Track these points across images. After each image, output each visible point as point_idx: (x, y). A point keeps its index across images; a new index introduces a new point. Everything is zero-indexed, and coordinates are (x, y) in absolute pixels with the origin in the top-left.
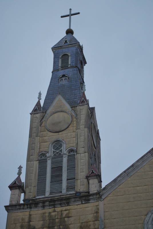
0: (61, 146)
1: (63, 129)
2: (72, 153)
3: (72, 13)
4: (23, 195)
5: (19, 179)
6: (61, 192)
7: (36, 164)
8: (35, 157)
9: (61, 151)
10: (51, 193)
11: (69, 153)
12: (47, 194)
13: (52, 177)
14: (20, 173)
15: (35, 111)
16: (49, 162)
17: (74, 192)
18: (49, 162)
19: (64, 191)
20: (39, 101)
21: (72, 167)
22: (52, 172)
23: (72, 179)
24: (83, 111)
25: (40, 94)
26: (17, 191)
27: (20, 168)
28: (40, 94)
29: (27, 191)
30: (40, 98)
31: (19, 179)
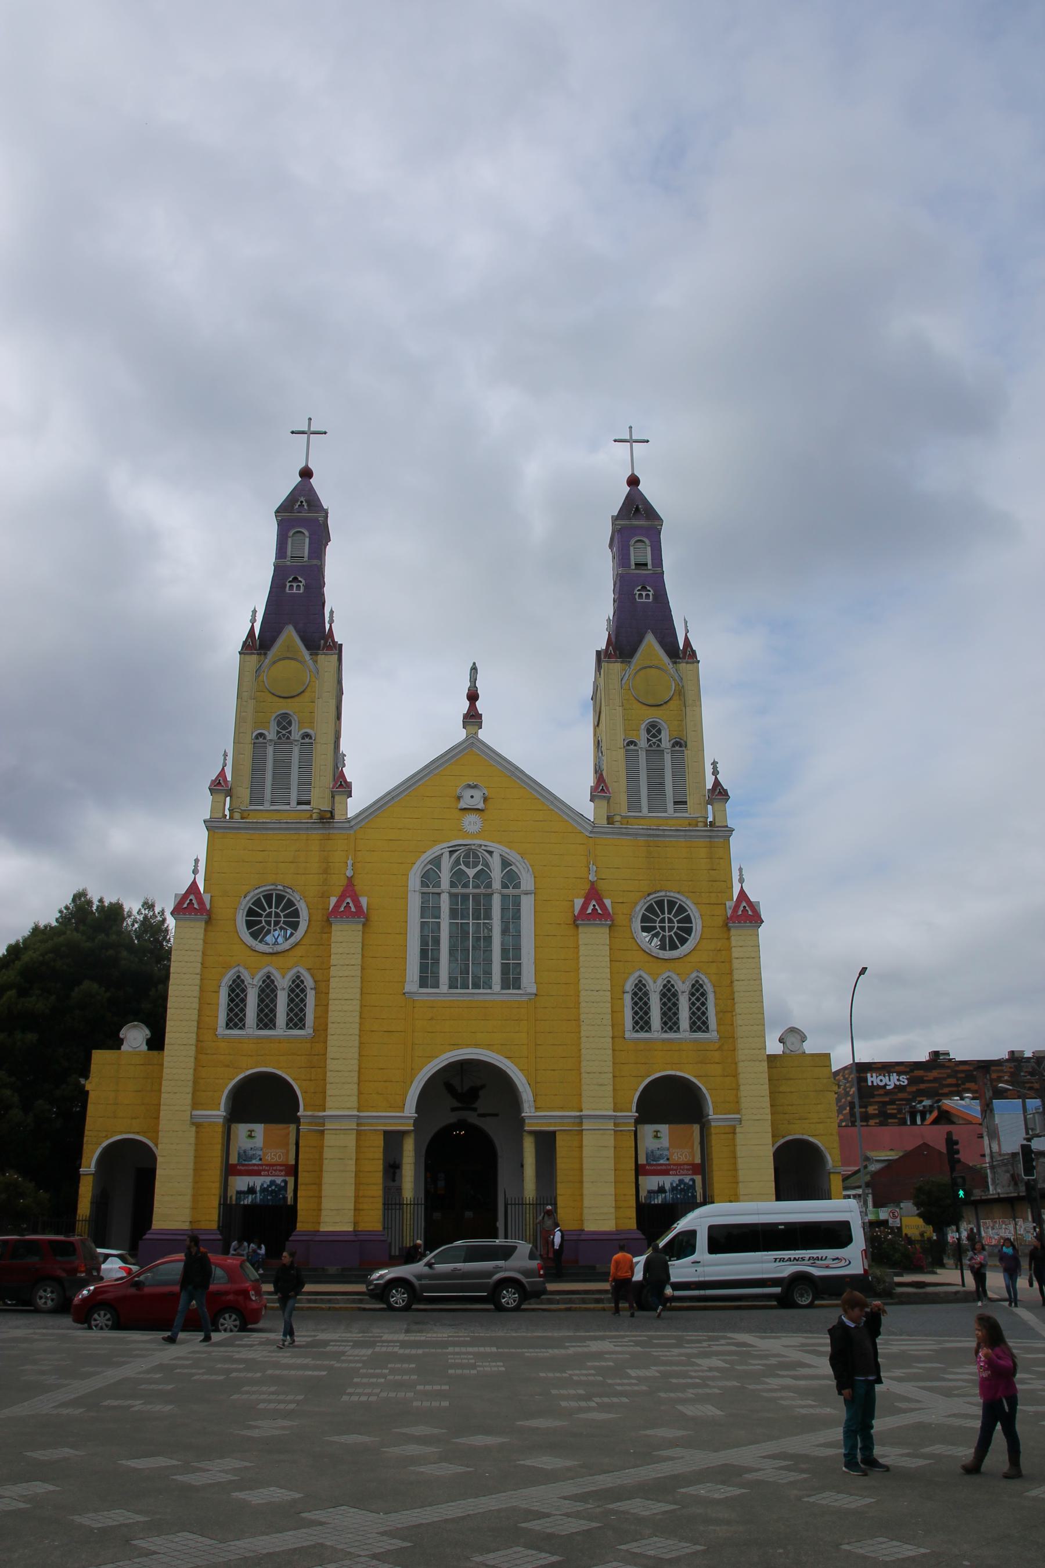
0: (290, 723)
1: (295, 694)
2: (307, 740)
3: (312, 429)
4: (228, 798)
5: (222, 773)
6: (289, 804)
7: (248, 749)
8: (248, 738)
11: (303, 738)
12: (267, 806)
16: (270, 750)
18: (270, 750)
20: (252, 628)
21: (306, 765)
22: (275, 767)
23: (305, 784)
24: (326, 660)
25: (254, 612)
26: (220, 797)
27: (225, 755)
28: (254, 612)
29: (234, 791)
30: (253, 621)
31: (222, 773)
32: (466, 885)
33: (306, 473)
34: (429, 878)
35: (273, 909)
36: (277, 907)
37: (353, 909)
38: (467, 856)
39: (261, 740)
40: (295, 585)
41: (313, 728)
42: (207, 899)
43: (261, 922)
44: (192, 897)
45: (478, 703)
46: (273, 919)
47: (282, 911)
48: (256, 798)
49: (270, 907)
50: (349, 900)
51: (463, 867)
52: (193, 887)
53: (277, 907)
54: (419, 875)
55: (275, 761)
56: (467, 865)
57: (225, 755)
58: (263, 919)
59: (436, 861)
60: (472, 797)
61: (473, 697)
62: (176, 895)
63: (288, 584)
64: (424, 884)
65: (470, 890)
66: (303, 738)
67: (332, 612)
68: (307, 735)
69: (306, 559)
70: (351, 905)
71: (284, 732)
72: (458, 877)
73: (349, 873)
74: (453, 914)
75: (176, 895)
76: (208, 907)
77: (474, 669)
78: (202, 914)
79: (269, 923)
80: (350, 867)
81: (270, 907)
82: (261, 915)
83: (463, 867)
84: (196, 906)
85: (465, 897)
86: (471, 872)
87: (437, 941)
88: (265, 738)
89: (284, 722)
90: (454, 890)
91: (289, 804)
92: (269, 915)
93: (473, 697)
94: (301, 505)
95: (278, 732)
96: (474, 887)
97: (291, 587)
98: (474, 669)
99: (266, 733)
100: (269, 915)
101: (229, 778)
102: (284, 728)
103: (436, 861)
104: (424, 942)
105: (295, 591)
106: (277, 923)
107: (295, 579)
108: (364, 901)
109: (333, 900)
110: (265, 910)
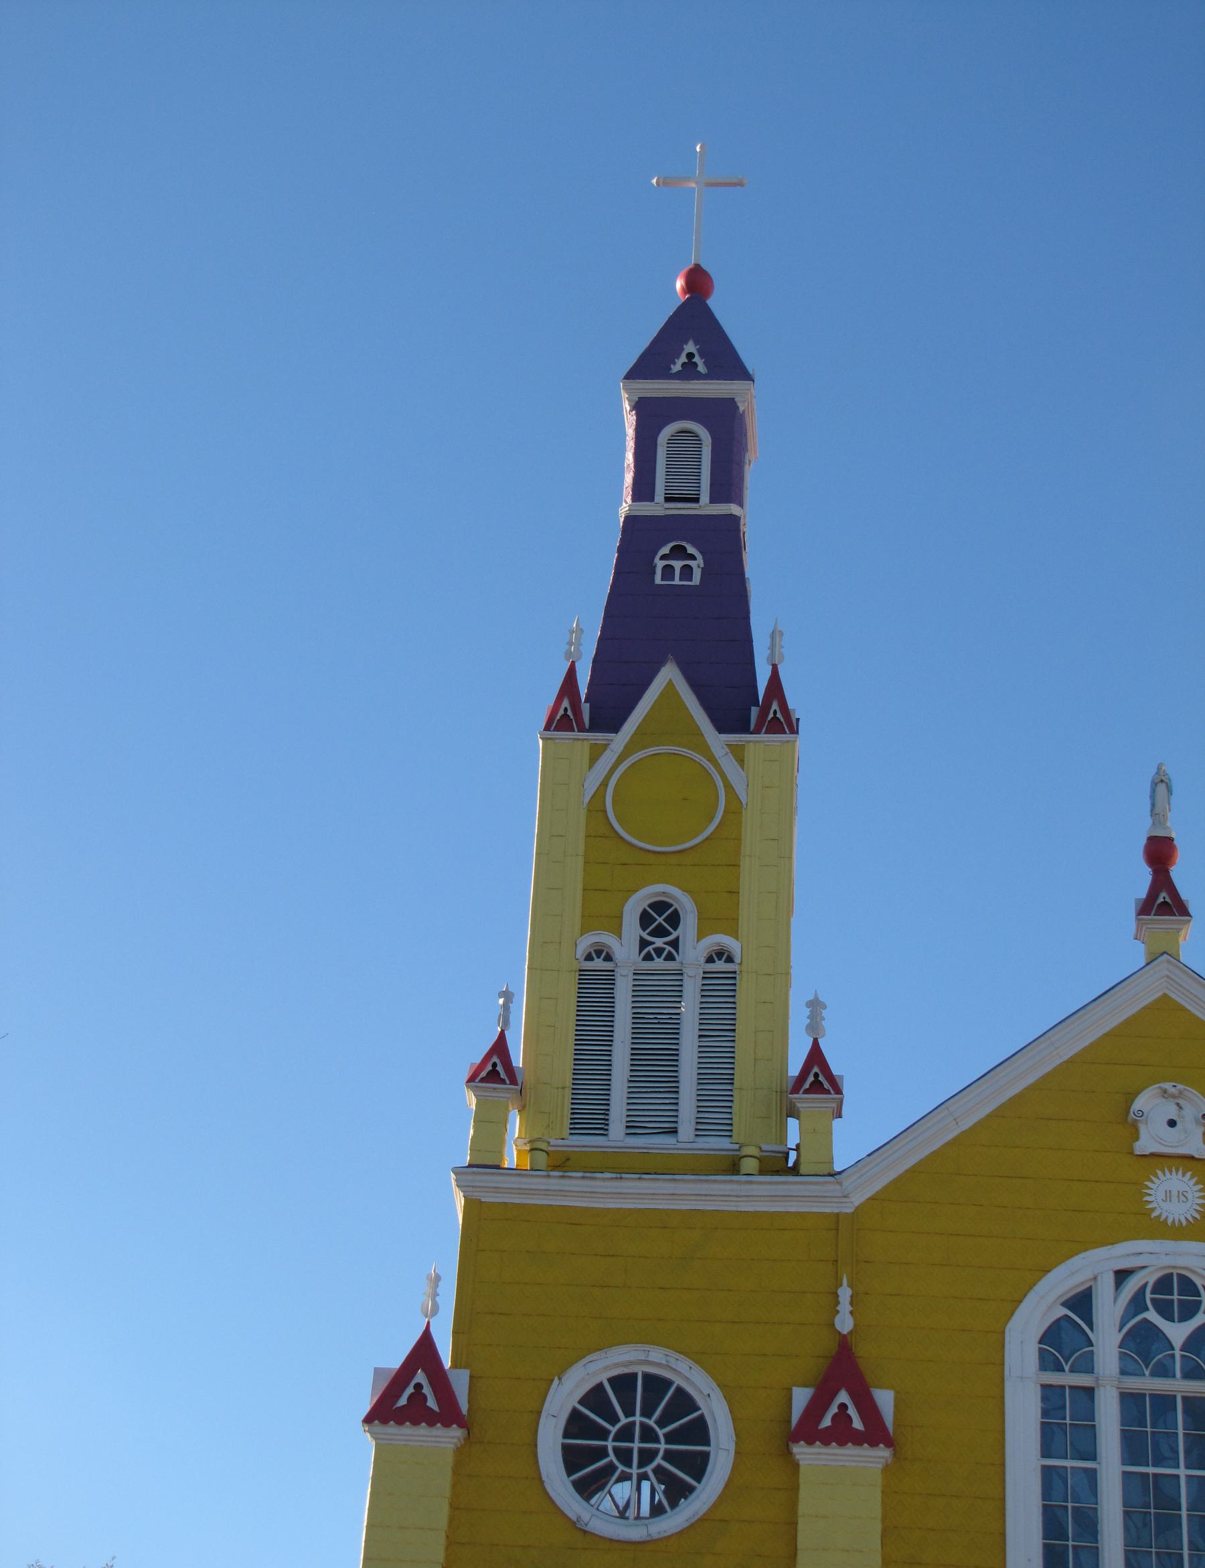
0: (674, 919)
2: (720, 965)
5: (500, 1047)
6: (674, 1131)
9: (675, 944)
10: (632, 1128)
13: (635, 1053)
14: (506, 1021)
15: (558, 723)
17: (724, 1143)
19: (686, 1129)
21: (720, 1028)
22: (637, 1033)
23: (718, 1078)
27: (508, 996)
31: (500, 1047)
32: (1163, 1371)
33: (698, 282)
34: (1065, 1341)
35: (638, 1418)
36: (647, 1413)
37: (857, 1424)
38: (1164, 1284)
39: (598, 964)
40: (677, 565)
41: (735, 935)
42: (460, 1383)
43: (603, 1453)
44: (420, 1377)
45: (1178, 874)
46: (636, 1445)
47: (662, 1423)
48: (589, 1116)
49: (629, 1412)
50: (843, 1397)
51: (1152, 1316)
52: (425, 1349)
53: (647, 1413)
54: (1037, 1328)
55: (636, 1017)
56: (1165, 1310)
57: (508, 996)
58: (610, 1444)
59: (1082, 1303)
60: (1172, 1123)
61: (1160, 853)
62: (378, 1372)
63: (660, 564)
64: (1048, 1363)
65: (1179, 1386)
66: (710, 960)
67: (774, 635)
68: (721, 954)
69: (705, 497)
70: (852, 1411)
71: (659, 942)
72: (1142, 1343)
73: (845, 1323)
74: (1133, 1448)
75: (378, 1372)
76: (464, 1407)
77: (1161, 782)
78: (447, 1425)
79: (625, 1456)
80: (845, 1306)
81: (629, 1412)
82: (604, 1434)
83: (1152, 1316)
84: (432, 1403)
85: (1164, 1403)
86: (1177, 1333)
87: (1089, 1524)
88: (608, 958)
89: (660, 920)
90: (1136, 1384)
91: (674, 1131)
92: (626, 1434)
93: (1160, 853)
94: (690, 365)
95: (644, 944)
96: (1187, 1375)
97: (668, 572)
98: (1161, 782)
99: (608, 939)
100: (626, 1434)
101: (518, 1060)
102: (660, 932)
103: (1082, 1303)
104: (1052, 1525)
105: (677, 581)
106: (647, 1457)
107: (678, 552)
108: (885, 1399)
109: (801, 1397)
110: (614, 1419)
